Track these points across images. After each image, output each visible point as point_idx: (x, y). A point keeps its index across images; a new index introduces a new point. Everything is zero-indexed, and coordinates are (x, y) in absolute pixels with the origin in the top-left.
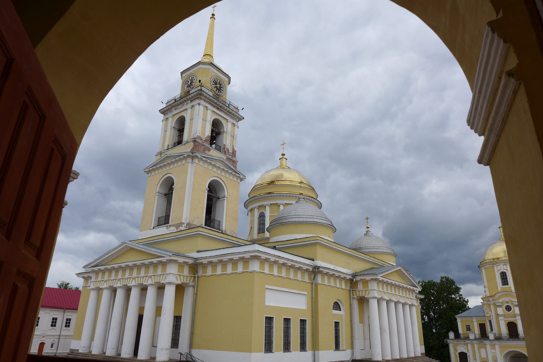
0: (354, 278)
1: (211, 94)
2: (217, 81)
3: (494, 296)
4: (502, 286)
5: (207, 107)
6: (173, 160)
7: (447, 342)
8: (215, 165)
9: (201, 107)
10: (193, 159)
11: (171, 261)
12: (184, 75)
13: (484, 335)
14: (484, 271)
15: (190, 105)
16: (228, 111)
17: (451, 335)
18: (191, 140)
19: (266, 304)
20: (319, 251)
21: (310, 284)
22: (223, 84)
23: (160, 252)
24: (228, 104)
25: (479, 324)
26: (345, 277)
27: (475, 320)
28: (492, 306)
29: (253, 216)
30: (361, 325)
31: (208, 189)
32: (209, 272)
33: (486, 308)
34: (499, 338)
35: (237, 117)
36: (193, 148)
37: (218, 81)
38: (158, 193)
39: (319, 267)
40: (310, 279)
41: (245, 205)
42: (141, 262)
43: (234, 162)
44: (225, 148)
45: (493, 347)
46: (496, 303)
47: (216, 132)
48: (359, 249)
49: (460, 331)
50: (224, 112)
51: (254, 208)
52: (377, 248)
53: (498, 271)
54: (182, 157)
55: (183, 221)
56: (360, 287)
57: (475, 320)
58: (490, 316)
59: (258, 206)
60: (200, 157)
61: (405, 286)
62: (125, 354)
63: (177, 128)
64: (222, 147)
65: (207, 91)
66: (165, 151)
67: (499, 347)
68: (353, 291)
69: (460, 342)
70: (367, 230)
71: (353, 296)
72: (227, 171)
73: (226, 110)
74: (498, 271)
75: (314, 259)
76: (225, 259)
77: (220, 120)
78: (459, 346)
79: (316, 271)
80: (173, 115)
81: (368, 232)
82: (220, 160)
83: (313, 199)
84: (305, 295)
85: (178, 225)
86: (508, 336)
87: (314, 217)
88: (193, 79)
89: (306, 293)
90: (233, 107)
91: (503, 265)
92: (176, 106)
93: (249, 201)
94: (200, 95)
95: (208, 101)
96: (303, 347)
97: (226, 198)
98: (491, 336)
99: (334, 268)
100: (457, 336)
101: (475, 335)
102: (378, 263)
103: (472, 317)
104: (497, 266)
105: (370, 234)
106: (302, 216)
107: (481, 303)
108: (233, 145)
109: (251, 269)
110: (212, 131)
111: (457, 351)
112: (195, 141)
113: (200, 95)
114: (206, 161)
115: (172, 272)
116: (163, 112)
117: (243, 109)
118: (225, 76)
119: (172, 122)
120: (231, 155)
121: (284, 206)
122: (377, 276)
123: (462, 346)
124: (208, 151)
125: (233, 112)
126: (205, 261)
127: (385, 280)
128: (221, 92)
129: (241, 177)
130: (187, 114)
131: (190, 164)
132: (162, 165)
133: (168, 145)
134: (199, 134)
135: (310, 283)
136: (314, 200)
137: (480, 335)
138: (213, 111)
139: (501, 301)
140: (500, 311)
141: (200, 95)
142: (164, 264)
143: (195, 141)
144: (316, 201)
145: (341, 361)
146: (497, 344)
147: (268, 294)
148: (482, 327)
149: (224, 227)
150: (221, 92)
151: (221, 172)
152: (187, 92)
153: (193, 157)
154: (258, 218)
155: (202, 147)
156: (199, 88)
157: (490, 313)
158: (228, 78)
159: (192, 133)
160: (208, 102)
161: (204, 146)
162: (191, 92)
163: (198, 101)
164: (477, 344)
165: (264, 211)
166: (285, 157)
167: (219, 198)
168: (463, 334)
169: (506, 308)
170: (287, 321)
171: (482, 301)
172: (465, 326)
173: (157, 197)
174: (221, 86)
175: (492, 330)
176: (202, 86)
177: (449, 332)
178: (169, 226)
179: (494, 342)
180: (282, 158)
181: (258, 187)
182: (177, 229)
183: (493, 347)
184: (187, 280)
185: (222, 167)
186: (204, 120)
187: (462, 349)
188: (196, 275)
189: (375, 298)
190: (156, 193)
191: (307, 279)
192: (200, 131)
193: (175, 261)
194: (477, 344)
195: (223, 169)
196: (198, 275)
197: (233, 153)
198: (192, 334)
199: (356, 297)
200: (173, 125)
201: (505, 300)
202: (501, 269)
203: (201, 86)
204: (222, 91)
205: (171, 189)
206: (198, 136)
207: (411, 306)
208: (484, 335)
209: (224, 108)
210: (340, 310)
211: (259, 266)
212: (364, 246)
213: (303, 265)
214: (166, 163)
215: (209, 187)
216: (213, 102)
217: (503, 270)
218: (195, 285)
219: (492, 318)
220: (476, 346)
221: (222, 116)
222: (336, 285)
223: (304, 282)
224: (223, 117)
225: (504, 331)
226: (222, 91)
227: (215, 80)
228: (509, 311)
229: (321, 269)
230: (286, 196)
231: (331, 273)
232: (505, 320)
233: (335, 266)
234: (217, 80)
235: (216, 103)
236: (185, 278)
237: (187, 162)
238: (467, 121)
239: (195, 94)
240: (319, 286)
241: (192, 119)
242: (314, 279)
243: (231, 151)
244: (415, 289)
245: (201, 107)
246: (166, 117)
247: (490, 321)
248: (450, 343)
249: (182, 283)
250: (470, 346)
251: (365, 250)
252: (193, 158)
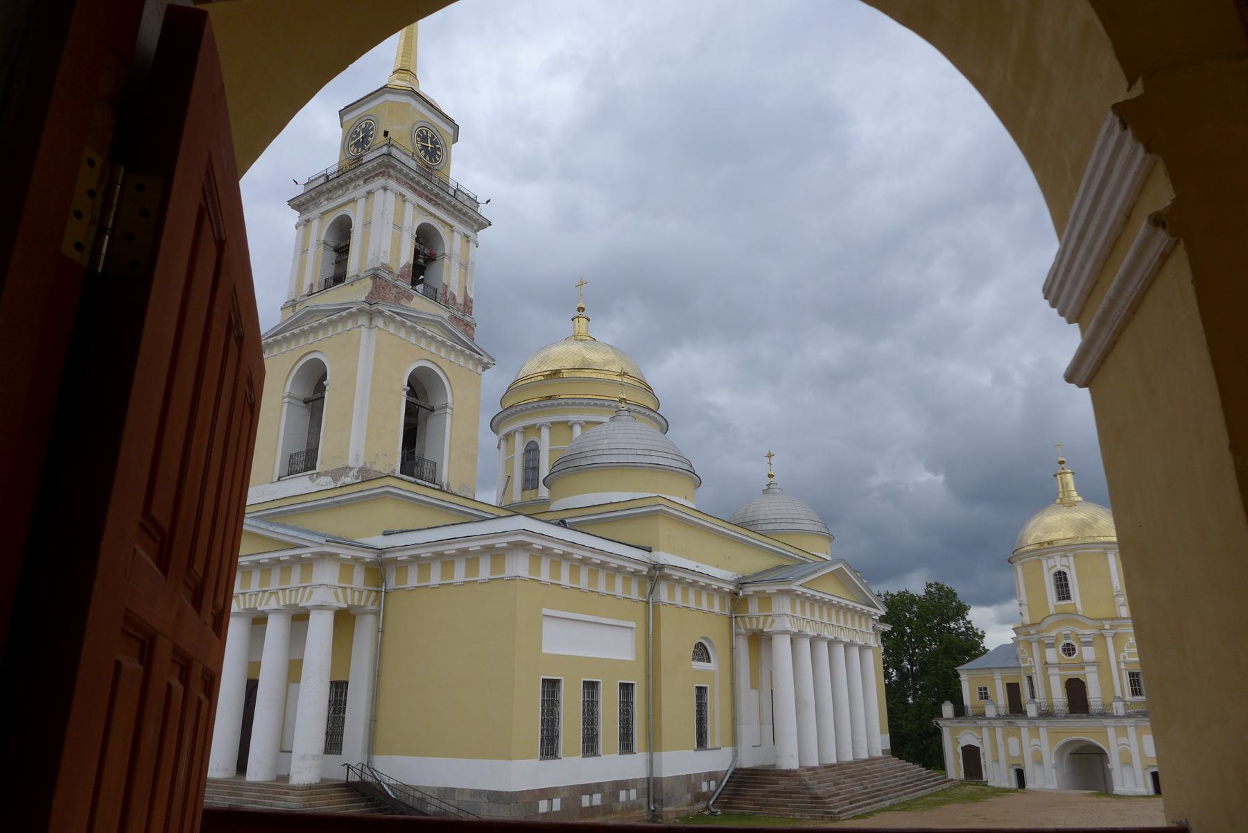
0: (741, 589)
1: (413, 164)
2: (427, 133)
3: (1039, 624)
4: (1057, 601)
5: (404, 196)
6: (325, 320)
7: (938, 725)
8: (423, 334)
9: (390, 196)
10: (371, 319)
11: (322, 556)
12: (346, 118)
13: (1016, 706)
14: (1019, 569)
15: (362, 191)
16: (454, 207)
17: (948, 709)
18: (368, 273)
19: (544, 651)
20: (664, 529)
21: (642, 605)
22: (442, 141)
23: (295, 535)
24: (452, 189)
25: (1007, 684)
26: (720, 588)
27: (997, 676)
28: (1035, 646)
29: (510, 450)
30: (754, 693)
31: (409, 388)
32: (413, 579)
33: (1022, 650)
34: (1047, 714)
35: (475, 221)
36: (371, 293)
37: (430, 135)
38: (289, 396)
39: (662, 567)
40: (642, 592)
41: (494, 422)
42: (252, 558)
43: (468, 327)
44: (446, 292)
45: (1035, 733)
46: (1043, 639)
47: (425, 255)
48: (751, 523)
49: (967, 701)
50: (445, 209)
51: (514, 433)
52: (791, 521)
53: (1050, 569)
54: (344, 313)
55: (351, 463)
56: (754, 608)
57: (997, 676)
58: (1030, 668)
59: (523, 427)
60: (388, 313)
61: (851, 604)
62: (217, 770)
63: (332, 244)
64: (440, 291)
65: (404, 158)
66: (303, 299)
67: (1048, 733)
68: (739, 619)
69: (965, 724)
70: (769, 480)
71: (738, 630)
72: (452, 348)
73: (449, 203)
74: (1050, 569)
75: (651, 548)
76: (450, 549)
77: (435, 226)
78: (962, 733)
79: (656, 575)
80: (323, 214)
81: (772, 486)
82: (436, 322)
83: (648, 412)
84: (632, 628)
85: (337, 474)
86: (1067, 710)
87: (652, 453)
88: (369, 127)
89: (633, 624)
90: (465, 197)
91: (1062, 556)
92: (330, 191)
93: (501, 415)
94: (386, 166)
95: (406, 180)
96: (626, 745)
97: (448, 410)
98: (1031, 710)
99: (697, 567)
100: (960, 711)
101: (997, 708)
102: (793, 555)
103: (993, 670)
104: (1049, 558)
105: (777, 491)
106: (625, 452)
107: (1012, 638)
108: (466, 287)
109: (508, 573)
111: (959, 743)
112: (375, 276)
113: (387, 167)
114: (403, 324)
115: (327, 581)
116: (298, 204)
117: (489, 201)
118: (447, 123)
119: (320, 230)
120: (462, 308)
121: (582, 427)
122: (790, 584)
123: (971, 733)
124: (407, 302)
125: (465, 209)
126: (402, 556)
127: (809, 592)
128: (436, 161)
129: (485, 360)
130: (355, 213)
131: (364, 330)
132: (297, 331)
133: (312, 285)
134: (387, 261)
135: (641, 603)
136: (652, 414)
137: (1008, 709)
138: (419, 206)
139: (1053, 633)
140: (1052, 655)
141: (387, 167)
142: (306, 564)
143: (375, 276)
144: (656, 416)
145: (710, 772)
146: (1043, 727)
147: (548, 628)
148: (1013, 690)
149: (445, 476)
150: (436, 161)
151: (438, 349)
152: (355, 157)
153: (371, 314)
154: (523, 454)
155: (394, 290)
156: (385, 150)
157: (1030, 661)
158: (452, 127)
159: (370, 257)
160: (405, 184)
161: (397, 287)
162: (365, 159)
163: (380, 182)
164: (1002, 727)
165: (536, 439)
166: (584, 314)
167: (432, 410)
168: (972, 707)
169: (1064, 650)
170: (591, 687)
171: (1015, 635)
172: (977, 689)
173: (285, 407)
174: (437, 146)
175: (1033, 696)
176: (392, 145)
177: (943, 702)
178: (315, 475)
179: (1037, 723)
180: (578, 317)
181: (524, 383)
182: (335, 481)
183: (1035, 733)
184: (360, 599)
185: (439, 338)
186: (398, 227)
187: (968, 739)
188: (382, 587)
189: (786, 632)
190: (284, 398)
191: (635, 594)
192: (388, 254)
193: (334, 557)
194: (1002, 727)
195: (443, 343)
196: (387, 588)
197: (465, 304)
198: (373, 720)
199: (743, 631)
200: (323, 238)
201: (1064, 633)
202: (1055, 566)
203: (390, 145)
204: (438, 159)
205: (319, 388)
206: (383, 264)
207: (862, 648)
208: (1016, 706)
209: (443, 199)
210: (710, 662)
211: (528, 565)
212: (761, 517)
213: (629, 561)
214: (306, 327)
215: (409, 384)
216: (418, 183)
217: (1059, 568)
218: (380, 610)
219: (1034, 671)
220: (999, 732)
221: (439, 218)
222: (701, 604)
223: (630, 601)
224: (443, 221)
225: (1059, 697)
226: (438, 158)
227: (421, 131)
228: (1070, 655)
229: (667, 571)
230: (588, 404)
231: (690, 578)
232: (1060, 675)
233: (698, 564)
234: (427, 131)
235: (424, 187)
236: (357, 594)
237: (359, 324)
238: (1044, 289)
239: (375, 163)
240: (662, 607)
241: (367, 224)
242: (651, 592)
243: (460, 300)
244: (873, 610)
245: (390, 196)
246: (306, 217)
247: (1030, 678)
248: (945, 726)
249: (348, 605)
250: (985, 732)
251: (764, 527)
252: (371, 316)
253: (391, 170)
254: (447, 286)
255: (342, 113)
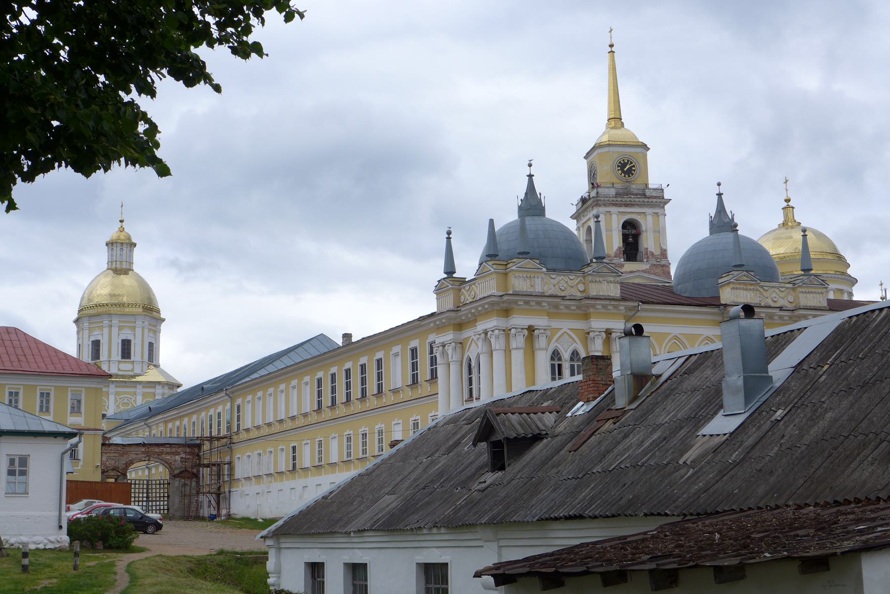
44: (647, 252)
80: (583, 224)
110: (625, 237)
117: (669, 185)
128: (633, 174)
204: (633, 172)
226: (633, 172)
227: (620, 163)
253: (599, 202)
254: (647, 249)
255: (586, 158)
